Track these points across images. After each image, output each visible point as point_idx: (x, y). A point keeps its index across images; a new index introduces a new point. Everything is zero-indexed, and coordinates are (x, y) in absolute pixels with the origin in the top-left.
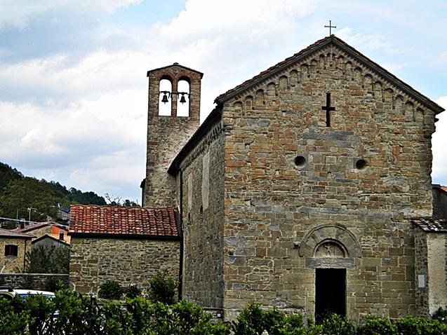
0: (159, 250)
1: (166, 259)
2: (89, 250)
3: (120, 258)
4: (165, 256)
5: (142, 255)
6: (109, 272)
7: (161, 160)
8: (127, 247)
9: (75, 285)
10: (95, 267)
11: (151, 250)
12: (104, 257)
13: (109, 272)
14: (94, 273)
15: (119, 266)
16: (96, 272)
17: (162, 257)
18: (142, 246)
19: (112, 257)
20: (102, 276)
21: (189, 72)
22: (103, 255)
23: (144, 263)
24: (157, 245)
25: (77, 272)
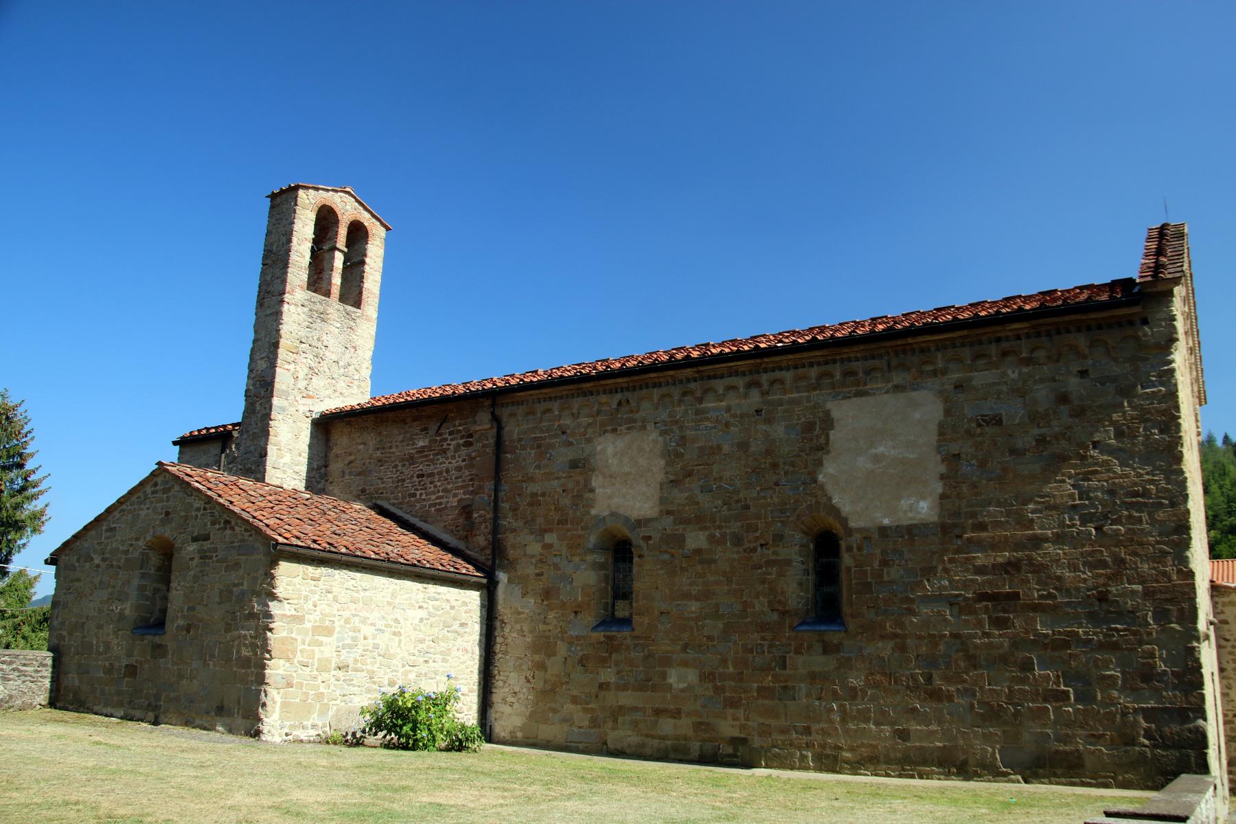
0: (452, 608)
1: (461, 630)
2: (317, 597)
3: (380, 624)
4: (462, 625)
5: (421, 620)
6: (356, 661)
7: (302, 384)
8: (393, 595)
9: (278, 698)
10: (328, 649)
11: (437, 609)
12: (347, 621)
13: (356, 661)
14: (323, 667)
15: (376, 647)
16: (328, 661)
17: (456, 627)
18: (421, 596)
19: (364, 621)
20: (340, 674)
21: (367, 215)
22: (346, 614)
23: (422, 641)
24: (448, 596)
25: (288, 659)
